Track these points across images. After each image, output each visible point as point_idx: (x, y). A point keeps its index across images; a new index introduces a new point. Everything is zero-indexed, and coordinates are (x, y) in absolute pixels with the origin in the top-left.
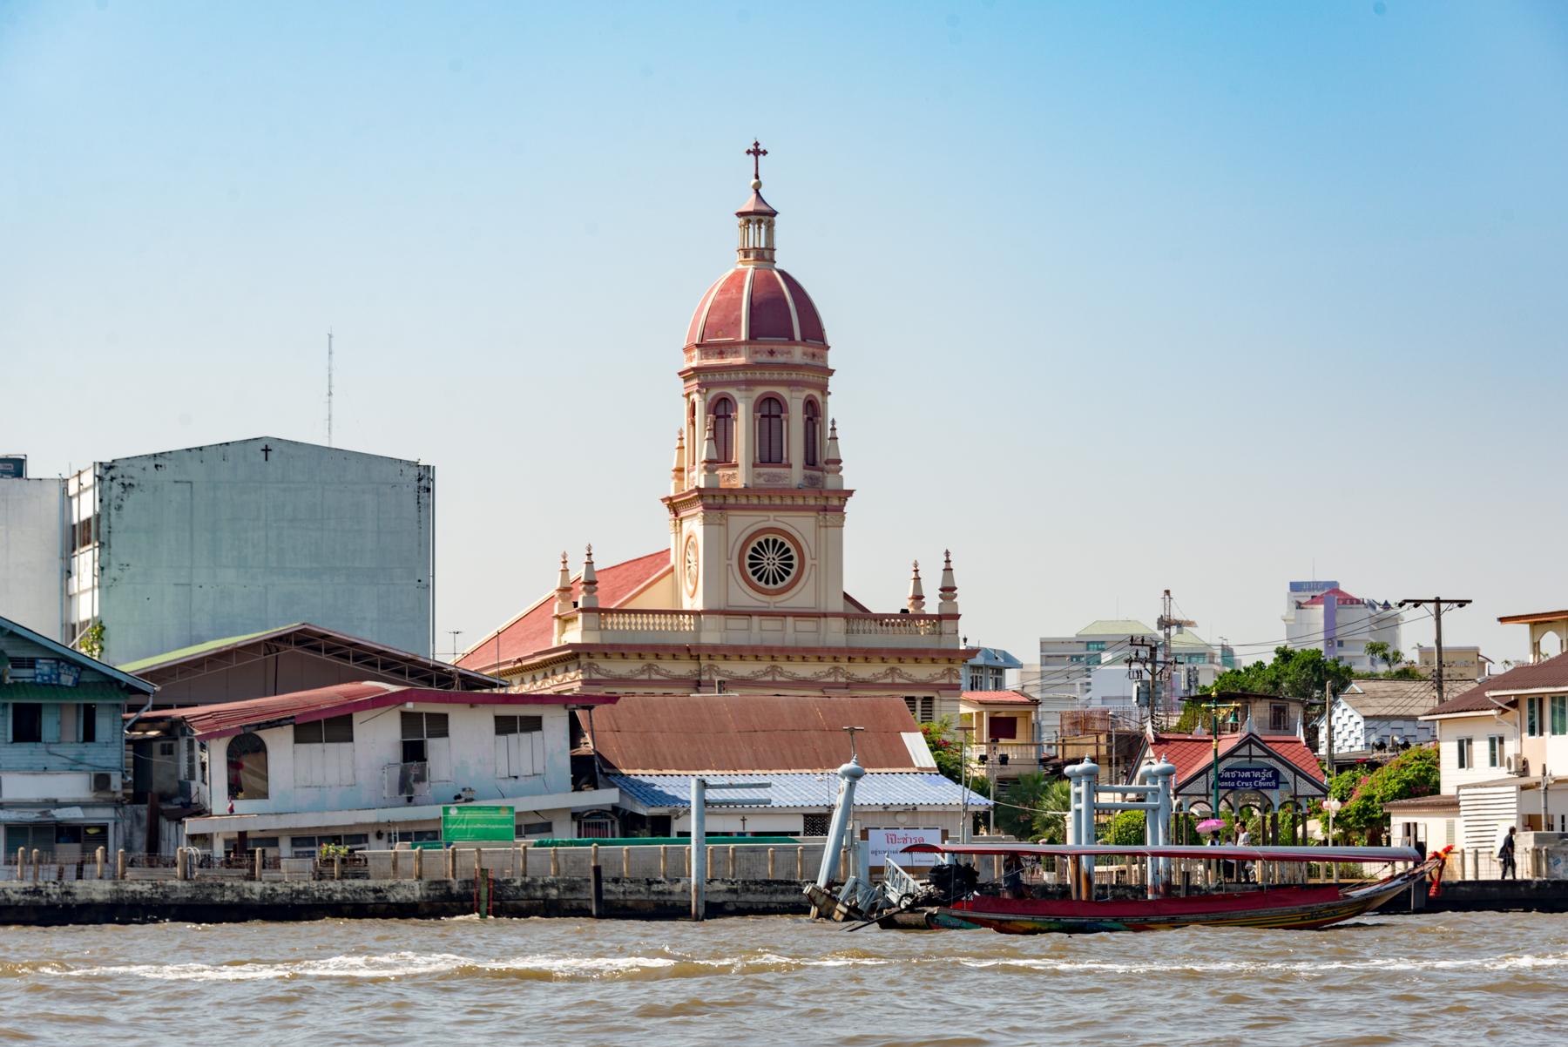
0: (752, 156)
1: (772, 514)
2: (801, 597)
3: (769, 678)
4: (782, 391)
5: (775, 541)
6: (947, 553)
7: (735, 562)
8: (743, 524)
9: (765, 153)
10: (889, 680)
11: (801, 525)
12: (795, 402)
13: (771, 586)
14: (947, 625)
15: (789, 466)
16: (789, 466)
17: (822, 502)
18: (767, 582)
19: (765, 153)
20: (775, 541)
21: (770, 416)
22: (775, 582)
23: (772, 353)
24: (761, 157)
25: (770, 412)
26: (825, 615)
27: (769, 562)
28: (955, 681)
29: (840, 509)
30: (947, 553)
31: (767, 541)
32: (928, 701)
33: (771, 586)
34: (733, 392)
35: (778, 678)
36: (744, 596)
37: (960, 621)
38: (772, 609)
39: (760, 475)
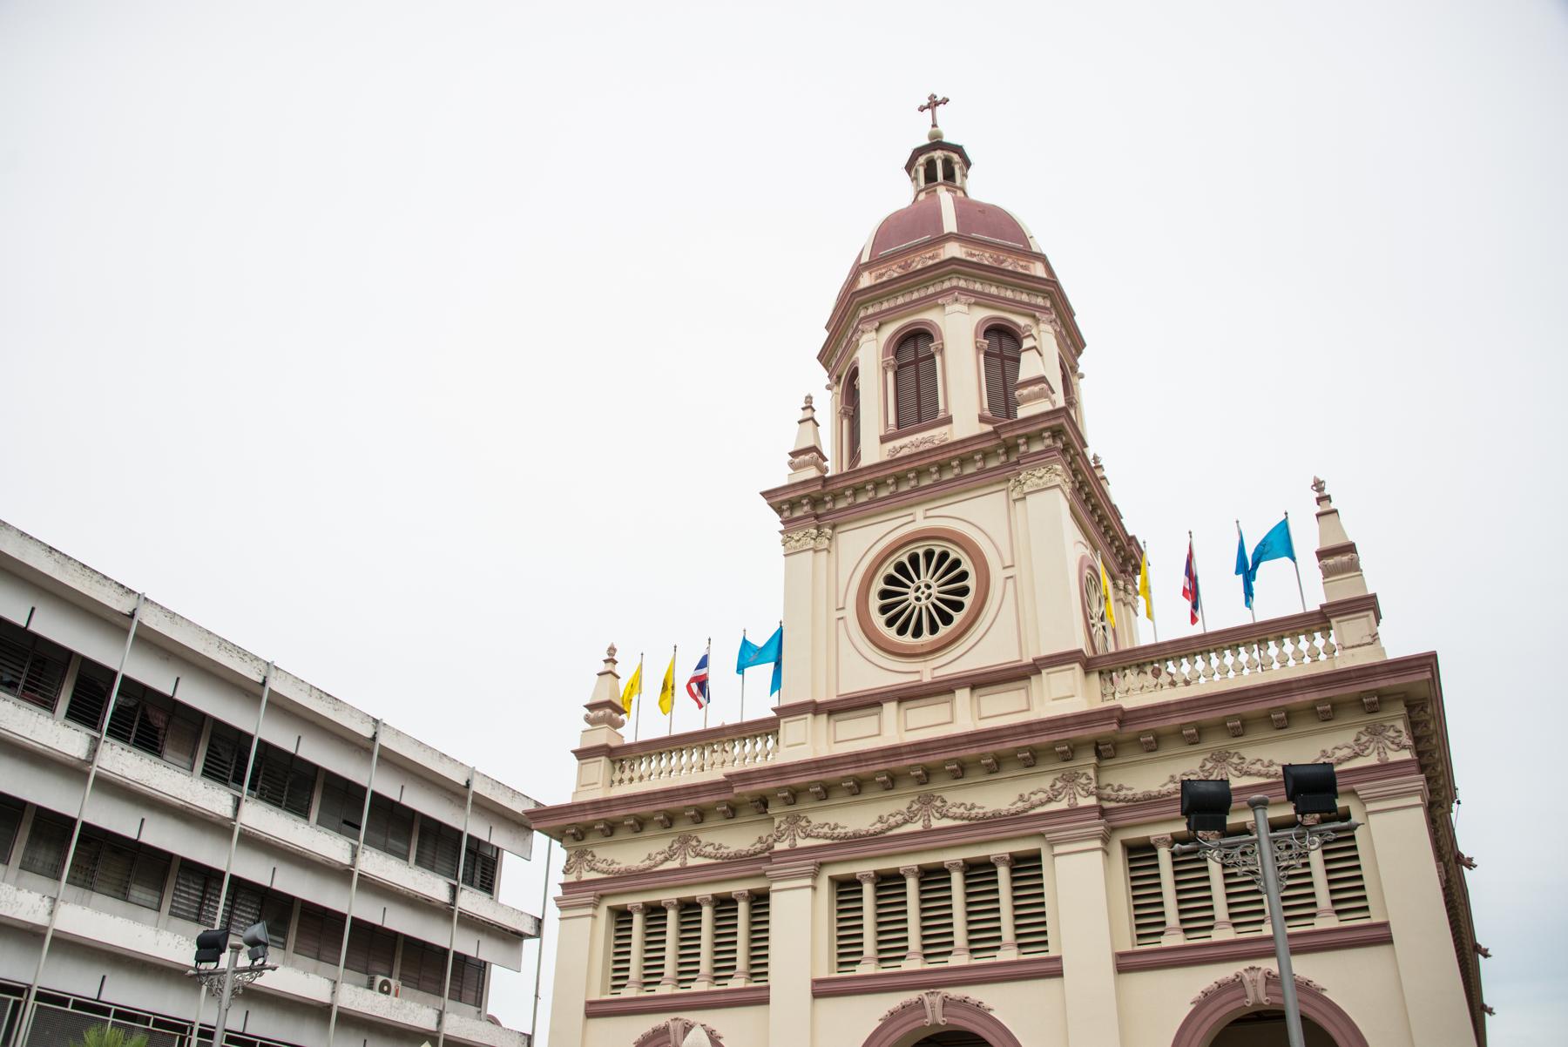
0: (928, 112)
1: (919, 512)
2: (988, 646)
3: (917, 826)
4: (931, 316)
6: (1318, 485)
8: (864, 542)
9: (945, 101)
12: (958, 328)
14: (1346, 630)
17: (1013, 459)
18: (917, 633)
19: (945, 101)
20: (929, 555)
21: (916, 362)
22: (934, 629)
24: (939, 109)
27: (926, 594)
30: (1318, 485)
33: (926, 637)
35: (936, 824)
38: (927, 679)
39: (896, 451)
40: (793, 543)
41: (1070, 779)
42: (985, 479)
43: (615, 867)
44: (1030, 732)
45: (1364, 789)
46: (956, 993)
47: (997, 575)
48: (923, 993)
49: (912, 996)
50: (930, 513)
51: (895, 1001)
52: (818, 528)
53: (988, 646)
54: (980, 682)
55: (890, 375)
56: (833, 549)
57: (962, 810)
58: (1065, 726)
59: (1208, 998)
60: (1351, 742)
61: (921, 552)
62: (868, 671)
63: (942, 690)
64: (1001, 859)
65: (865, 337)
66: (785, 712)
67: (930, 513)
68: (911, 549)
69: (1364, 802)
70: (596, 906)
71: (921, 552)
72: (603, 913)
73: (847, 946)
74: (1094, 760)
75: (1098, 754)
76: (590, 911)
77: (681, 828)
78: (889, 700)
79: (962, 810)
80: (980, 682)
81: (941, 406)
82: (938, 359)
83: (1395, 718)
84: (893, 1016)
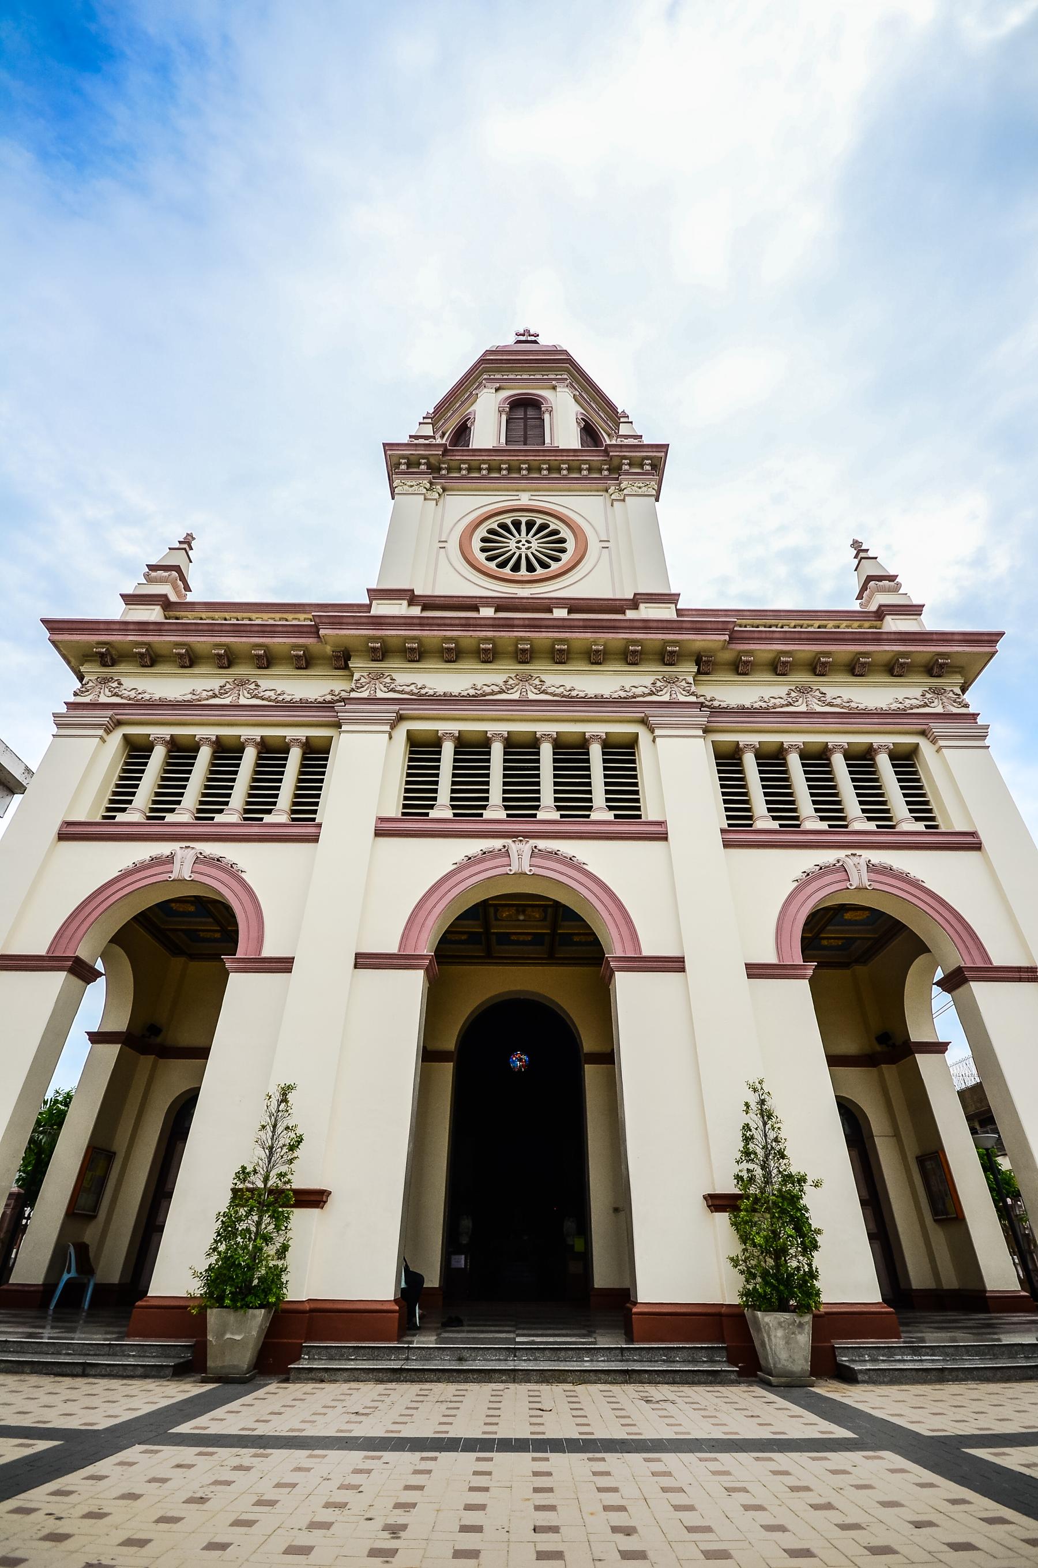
18: (516, 568)
32: (905, 761)
40: (405, 487)
41: (671, 681)
45: (937, 728)
46: (543, 844)
48: (509, 841)
49: (497, 844)
51: (475, 847)
52: (431, 483)
55: (504, 417)
56: (440, 503)
57: (561, 689)
59: (809, 878)
60: (918, 696)
61: (524, 520)
64: (596, 737)
68: (516, 516)
69: (934, 742)
70: (108, 731)
71: (524, 520)
72: (116, 739)
73: (418, 795)
75: (698, 662)
76: (101, 732)
77: (241, 671)
79: (561, 689)
82: (546, 417)
83: (954, 684)
84: (471, 861)
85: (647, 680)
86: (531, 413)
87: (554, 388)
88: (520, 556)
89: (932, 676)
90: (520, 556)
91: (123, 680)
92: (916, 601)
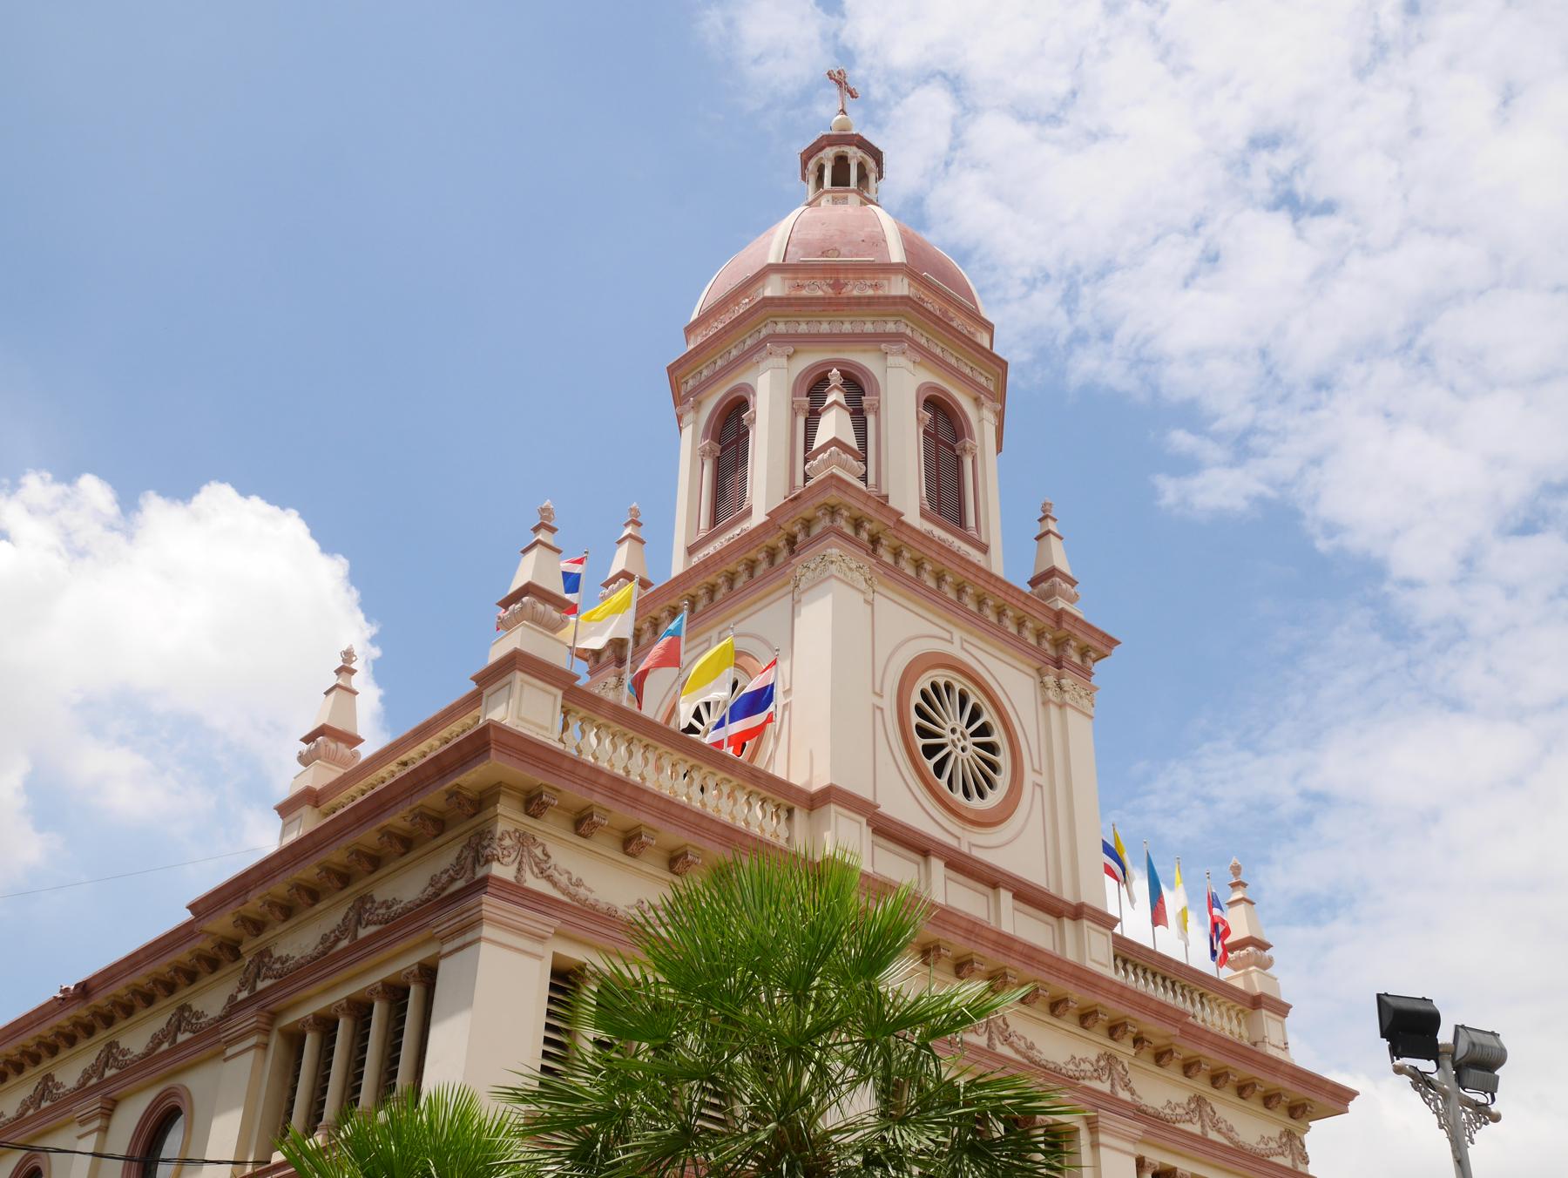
1: (958, 634)
5: (963, 699)
6: (1236, 870)
7: (889, 703)
10: (1196, 1129)
11: (1012, 681)
13: (959, 796)
15: (984, 549)
16: (984, 549)
23: (945, 313)
25: (943, 425)
26: (1078, 912)
28: (1301, 1168)
29: (1087, 674)
30: (1236, 870)
31: (948, 687)
34: (866, 360)
36: (906, 802)
37: (1290, 1020)
42: (1015, 643)
43: (592, 897)
44: (1120, 996)
47: (1029, 777)
50: (966, 646)
53: (1016, 849)
54: (1028, 896)
58: (1145, 1007)
61: (957, 687)
62: (906, 802)
63: (990, 879)
65: (902, 360)
66: (829, 795)
67: (966, 646)
74: (1132, 1052)
78: (940, 856)
80: (1028, 896)
81: (971, 522)
82: (968, 461)
85: (1093, 1058)
86: (944, 434)
87: (978, 402)
88: (948, 755)
89: (1292, 1116)
90: (948, 755)
91: (551, 849)
92: (1285, 999)
